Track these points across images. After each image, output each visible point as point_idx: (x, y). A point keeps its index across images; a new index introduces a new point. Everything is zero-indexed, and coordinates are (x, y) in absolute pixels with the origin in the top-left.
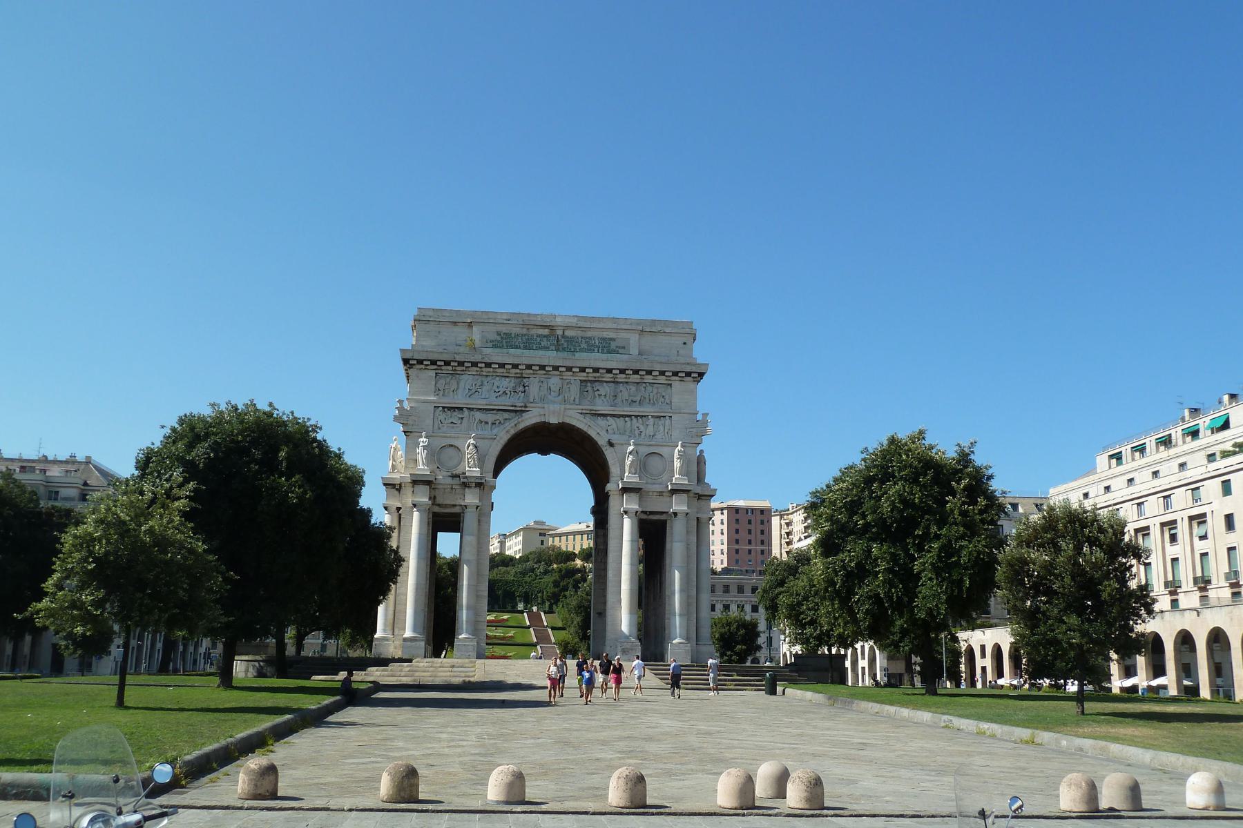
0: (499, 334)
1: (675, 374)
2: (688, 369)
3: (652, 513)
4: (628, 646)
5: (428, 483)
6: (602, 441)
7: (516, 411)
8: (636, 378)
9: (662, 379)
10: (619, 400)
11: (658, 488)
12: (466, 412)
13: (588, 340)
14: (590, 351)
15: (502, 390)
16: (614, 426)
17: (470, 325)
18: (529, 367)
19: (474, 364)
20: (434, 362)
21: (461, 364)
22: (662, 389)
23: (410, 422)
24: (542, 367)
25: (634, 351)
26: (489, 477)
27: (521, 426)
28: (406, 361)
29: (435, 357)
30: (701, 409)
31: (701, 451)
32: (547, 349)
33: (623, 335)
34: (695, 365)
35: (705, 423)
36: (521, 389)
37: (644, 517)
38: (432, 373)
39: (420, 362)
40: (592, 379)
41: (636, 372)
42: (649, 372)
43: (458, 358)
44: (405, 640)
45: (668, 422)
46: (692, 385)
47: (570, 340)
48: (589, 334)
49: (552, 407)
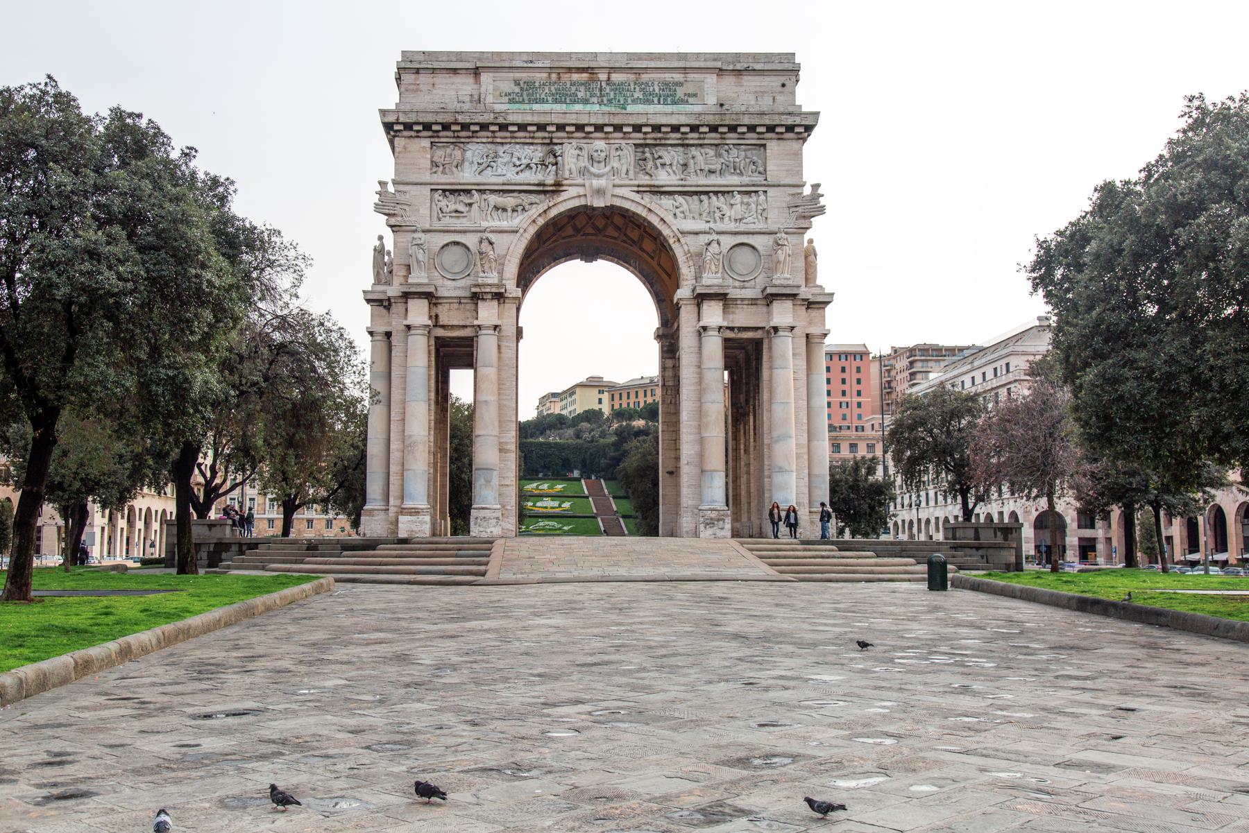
0: (517, 83)
2: (790, 121)
4: (714, 515)
7: (545, 192)
8: (712, 138)
9: (752, 138)
10: (691, 168)
11: (748, 293)
13: (643, 86)
14: (650, 102)
15: (524, 161)
16: (685, 207)
18: (561, 127)
19: (484, 127)
20: (427, 127)
21: (465, 127)
22: (754, 155)
23: (398, 210)
24: (580, 127)
25: (712, 100)
26: (512, 289)
27: (553, 213)
28: (388, 127)
29: (429, 118)
30: (809, 177)
31: (811, 241)
33: (691, 76)
34: (800, 114)
35: (815, 196)
36: (552, 160)
38: (426, 143)
39: (408, 126)
40: (651, 139)
41: (714, 129)
42: (733, 128)
43: (461, 119)
45: (762, 197)
46: (795, 145)
47: (619, 88)
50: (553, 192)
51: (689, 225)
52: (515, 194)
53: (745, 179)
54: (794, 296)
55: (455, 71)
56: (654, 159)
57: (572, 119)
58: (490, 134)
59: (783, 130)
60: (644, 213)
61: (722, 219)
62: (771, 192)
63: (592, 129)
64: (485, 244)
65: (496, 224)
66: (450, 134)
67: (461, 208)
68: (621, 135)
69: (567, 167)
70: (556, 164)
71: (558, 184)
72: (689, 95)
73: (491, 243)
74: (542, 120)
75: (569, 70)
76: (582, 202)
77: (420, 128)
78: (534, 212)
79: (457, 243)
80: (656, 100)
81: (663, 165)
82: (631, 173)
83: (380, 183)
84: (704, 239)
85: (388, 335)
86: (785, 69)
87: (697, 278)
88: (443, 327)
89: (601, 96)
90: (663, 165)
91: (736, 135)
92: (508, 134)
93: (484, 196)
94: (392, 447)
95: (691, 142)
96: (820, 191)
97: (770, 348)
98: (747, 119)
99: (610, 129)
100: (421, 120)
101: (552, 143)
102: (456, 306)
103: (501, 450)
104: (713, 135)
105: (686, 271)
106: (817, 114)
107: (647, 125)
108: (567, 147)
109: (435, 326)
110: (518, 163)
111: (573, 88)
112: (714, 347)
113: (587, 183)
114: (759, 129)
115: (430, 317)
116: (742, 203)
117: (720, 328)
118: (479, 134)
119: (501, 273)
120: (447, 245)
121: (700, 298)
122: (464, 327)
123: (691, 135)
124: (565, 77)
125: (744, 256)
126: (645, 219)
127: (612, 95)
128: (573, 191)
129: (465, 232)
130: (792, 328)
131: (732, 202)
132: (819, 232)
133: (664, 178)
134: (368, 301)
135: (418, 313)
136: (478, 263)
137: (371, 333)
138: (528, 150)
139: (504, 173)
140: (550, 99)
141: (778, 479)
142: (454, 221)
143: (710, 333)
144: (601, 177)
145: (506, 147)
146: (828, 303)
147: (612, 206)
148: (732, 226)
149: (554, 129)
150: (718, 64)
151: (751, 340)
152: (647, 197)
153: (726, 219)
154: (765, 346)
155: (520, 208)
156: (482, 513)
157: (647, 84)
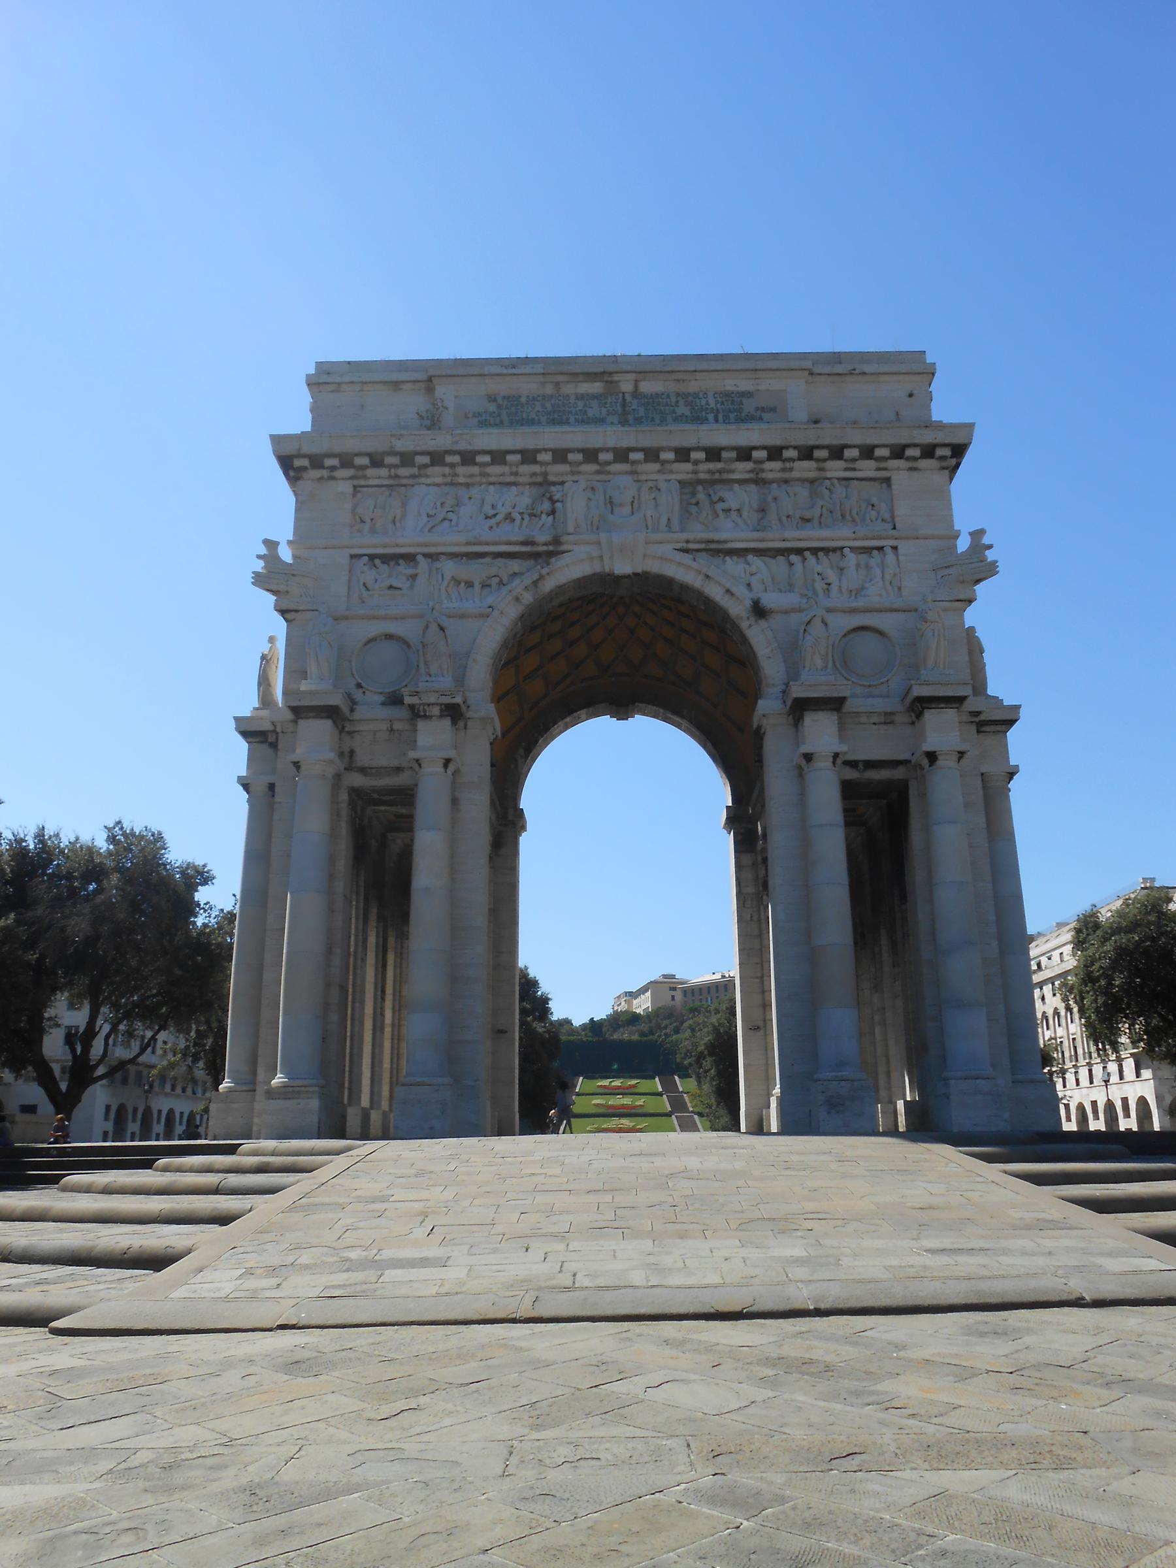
1: (898, 452)
2: (928, 438)
3: (870, 765)
5: (330, 712)
6: (737, 609)
7: (535, 556)
8: (804, 469)
9: (867, 468)
11: (880, 705)
12: (423, 563)
14: (697, 419)
15: (502, 511)
17: (429, 384)
18: (560, 456)
19: (437, 458)
20: (346, 461)
21: (407, 459)
24: (591, 455)
25: (801, 415)
27: (549, 585)
28: (286, 463)
29: (349, 445)
32: (601, 421)
36: (546, 506)
37: (851, 774)
38: (346, 487)
39: (316, 462)
41: (807, 453)
42: (837, 452)
43: (399, 446)
44: (271, 1094)
45: (890, 557)
46: (940, 478)
47: (651, 402)
48: (693, 387)
51: (770, 600)
52: (487, 560)
56: (713, 503)
58: (447, 470)
59: (916, 452)
63: (609, 456)
64: (434, 628)
66: (383, 472)
67: (396, 584)
68: (656, 466)
70: (553, 512)
71: (556, 541)
72: (763, 409)
73: (442, 629)
76: (597, 568)
77: (335, 462)
79: (389, 637)
80: (711, 417)
83: (268, 543)
85: (272, 787)
86: (915, 370)
87: (793, 674)
88: (363, 770)
89: (625, 413)
90: (727, 511)
91: (840, 464)
92: (476, 470)
93: (438, 565)
95: (770, 476)
96: (986, 540)
97: (923, 795)
98: (858, 444)
99: (639, 456)
100: (337, 449)
104: (806, 464)
105: (772, 669)
106: (970, 427)
107: (698, 449)
109: (348, 769)
110: (491, 512)
111: (580, 404)
114: (879, 452)
115: (341, 755)
116: (858, 566)
118: (430, 471)
119: (460, 680)
120: (373, 640)
121: (800, 708)
122: (398, 770)
123: (769, 465)
127: (642, 412)
129: (403, 618)
130: (961, 754)
131: (842, 565)
133: (731, 532)
134: (245, 734)
136: (422, 665)
137: (246, 787)
138: (511, 494)
140: (544, 419)
144: (627, 535)
145: (475, 491)
146: (1011, 722)
149: (546, 457)
150: (808, 364)
151: (888, 785)
152: (703, 559)
153: (834, 589)
155: (495, 581)
157: (696, 395)
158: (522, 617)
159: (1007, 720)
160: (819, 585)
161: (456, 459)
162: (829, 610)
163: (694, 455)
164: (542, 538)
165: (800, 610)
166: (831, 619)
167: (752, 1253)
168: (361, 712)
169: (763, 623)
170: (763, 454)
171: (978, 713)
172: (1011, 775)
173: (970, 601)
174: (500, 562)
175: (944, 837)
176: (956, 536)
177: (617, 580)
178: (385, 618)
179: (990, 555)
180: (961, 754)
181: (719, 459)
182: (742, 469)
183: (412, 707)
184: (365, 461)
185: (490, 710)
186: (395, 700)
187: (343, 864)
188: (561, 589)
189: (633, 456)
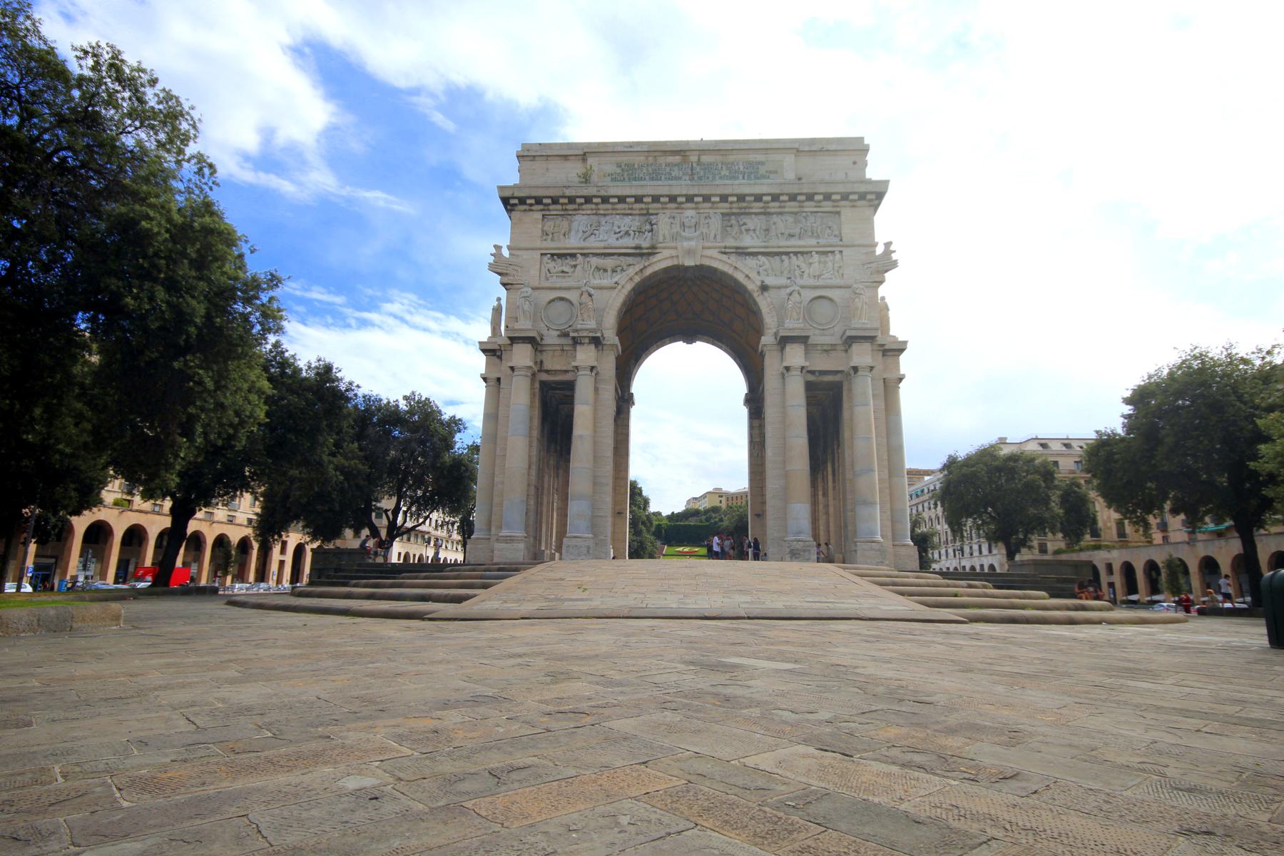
0: (619, 166)
2: (862, 189)
4: (799, 546)
5: (531, 340)
9: (827, 206)
10: (773, 233)
11: (828, 340)
18: (656, 199)
19: (588, 200)
20: (539, 201)
21: (572, 200)
24: (673, 199)
25: (790, 176)
27: (649, 272)
28: (505, 201)
30: (881, 237)
32: (677, 178)
36: (648, 227)
37: (811, 378)
38: (538, 215)
39: (522, 201)
41: (793, 198)
42: (810, 197)
43: (568, 192)
45: (838, 256)
47: (708, 167)
48: (731, 158)
49: (686, 244)
50: (650, 254)
51: (769, 281)
53: (822, 241)
54: (871, 339)
55: (565, 157)
57: (665, 191)
59: (855, 197)
60: (730, 271)
61: (802, 276)
62: (846, 252)
64: (585, 295)
65: (597, 282)
66: (559, 207)
67: (566, 269)
68: (709, 205)
69: (661, 233)
71: (653, 247)
74: (639, 192)
75: (665, 153)
76: (675, 262)
77: (532, 201)
78: (631, 271)
79: (562, 299)
81: (747, 230)
82: (719, 237)
83: (495, 246)
84: (784, 292)
85: (499, 379)
86: (856, 150)
87: (781, 323)
88: (547, 372)
90: (747, 230)
92: (609, 206)
94: (496, 480)
96: (892, 248)
97: (850, 390)
98: (820, 191)
99: (700, 199)
101: (648, 214)
102: (559, 353)
103: (595, 484)
104: (793, 204)
105: (770, 320)
106: (886, 183)
107: (732, 195)
108: (661, 217)
112: (796, 387)
113: (679, 245)
114: (834, 197)
115: (536, 363)
117: (803, 368)
119: (599, 323)
121: (784, 341)
122: (566, 371)
124: (662, 160)
125: (823, 309)
126: (731, 277)
127: (702, 173)
128: (666, 253)
129: (569, 289)
130: (872, 368)
132: (891, 289)
133: (748, 241)
134: (484, 351)
135: (522, 356)
137: (485, 379)
138: (628, 220)
139: (605, 238)
141: (862, 512)
142: (559, 280)
143: (794, 373)
146: (902, 350)
147: (700, 268)
148: (812, 282)
149: (649, 200)
150: (796, 146)
152: (733, 259)
153: (806, 275)
154: (845, 388)
156: (574, 542)
158: (633, 289)
159: (900, 349)
160: (797, 272)
161: (599, 200)
162: (802, 287)
163: (730, 199)
164: (645, 244)
165: (786, 287)
166: (802, 291)
167: (726, 600)
168: (547, 341)
169: (766, 294)
170: (769, 198)
171: (883, 345)
172: (901, 380)
173: (881, 282)
174: (622, 258)
175: (861, 412)
176: (876, 245)
177: (687, 268)
178: (560, 289)
179: (894, 256)
180: (872, 368)
181: (744, 201)
182: (757, 207)
183: (574, 338)
184: (549, 201)
185: (616, 340)
186: (565, 335)
187: (536, 422)
188: (655, 274)
189: (696, 199)
